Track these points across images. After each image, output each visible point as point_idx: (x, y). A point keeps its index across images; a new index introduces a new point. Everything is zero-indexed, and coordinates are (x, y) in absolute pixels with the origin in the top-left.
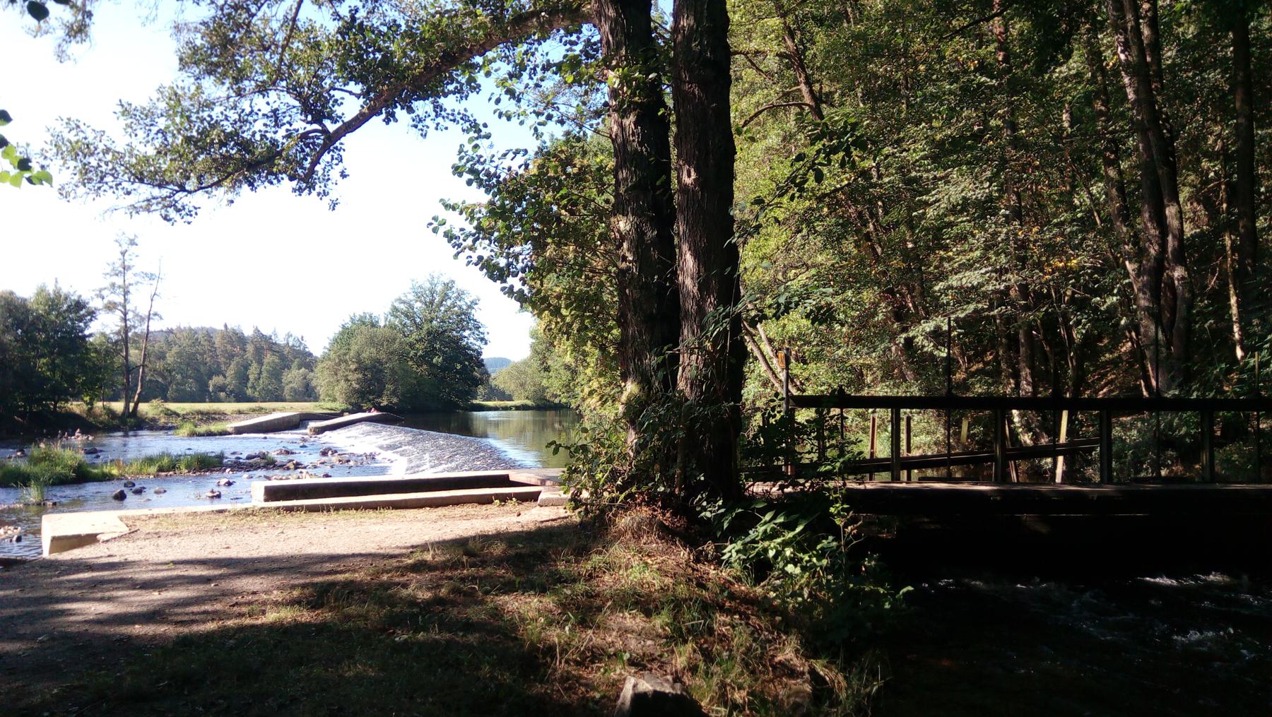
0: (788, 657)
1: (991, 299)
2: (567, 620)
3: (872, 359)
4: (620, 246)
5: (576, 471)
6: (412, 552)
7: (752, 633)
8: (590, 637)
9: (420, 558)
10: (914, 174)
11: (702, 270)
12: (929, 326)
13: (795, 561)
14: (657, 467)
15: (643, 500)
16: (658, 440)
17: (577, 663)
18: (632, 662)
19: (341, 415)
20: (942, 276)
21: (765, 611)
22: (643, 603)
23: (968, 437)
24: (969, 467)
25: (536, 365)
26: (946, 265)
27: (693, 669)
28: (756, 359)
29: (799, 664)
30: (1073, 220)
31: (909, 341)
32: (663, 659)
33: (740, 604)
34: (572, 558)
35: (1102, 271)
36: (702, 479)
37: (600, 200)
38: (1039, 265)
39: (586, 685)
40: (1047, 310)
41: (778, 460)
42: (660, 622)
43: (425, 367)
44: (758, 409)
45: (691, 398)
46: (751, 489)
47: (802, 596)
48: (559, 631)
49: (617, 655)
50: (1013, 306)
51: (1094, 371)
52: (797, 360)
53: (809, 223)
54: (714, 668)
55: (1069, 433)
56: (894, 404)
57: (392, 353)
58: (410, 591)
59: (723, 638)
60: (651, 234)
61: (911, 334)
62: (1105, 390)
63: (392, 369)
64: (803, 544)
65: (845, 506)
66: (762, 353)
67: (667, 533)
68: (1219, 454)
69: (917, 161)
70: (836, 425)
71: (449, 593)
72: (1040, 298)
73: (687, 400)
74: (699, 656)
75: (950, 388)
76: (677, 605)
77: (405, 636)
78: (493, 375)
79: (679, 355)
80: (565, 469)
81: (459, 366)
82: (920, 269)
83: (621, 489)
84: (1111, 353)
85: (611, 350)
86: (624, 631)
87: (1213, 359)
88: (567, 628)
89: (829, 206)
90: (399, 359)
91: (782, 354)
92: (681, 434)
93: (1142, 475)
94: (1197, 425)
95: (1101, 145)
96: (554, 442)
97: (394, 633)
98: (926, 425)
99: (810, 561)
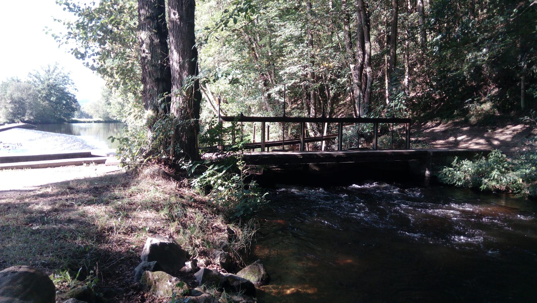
0: (218, 224)
1: (301, 78)
2: (119, 215)
3: (255, 102)
4: (141, 46)
5: (123, 150)
6: (41, 188)
7: (204, 215)
8: (131, 222)
9: (45, 191)
10: (271, 23)
11: (181, 58)
12: (277, 89)
13: (222, 185)
14: (162, 147)
15: (156, 162)
16: (162, 135)
17: (124, 233)
18: (151, 231)
19: (4, 124)
20: (282, 68)
21: (209, 206)
22: (155, 206)
23: (291, 134)
24: (291, 146)
25: (104, 102)
26: (284, 63)
27: (178, 232)
28: (206, 101)
29: (223, 226)
30: (332, 47)
31: (269, 95)
32: (164, 229)
33: (199, 204)
34: (122, 188)
35: (341, 68)
36: (182, 152)
37: (132, 24)
38: (319, 65)
39: (128, 243)
40: (321, 84)
41: (215, 143)
42: (163, 214)
43: (47, 102)
44: (207, 123)
45: (177, 116)
46: (204, 156)
47: (225, 199)
48: (115, 220)
49: (143, 229)
50: (309, 81)
51: (337, 108)
52: (224, 102)
53: (229, 42)
54: (188, 231)
55: (327, 131)
56: (263, 120)
57: (29, 95)
58: (40, 206)
59: (191, 218)
60: (157, 41)
61: (270, 92)
62: (340, 115)
63: (30, 103)
64: (226, 178)
65: (243, 162)
66: (209, 99)
67: (166, 176)
68: (379, 139)
69: (273, 17)
70: (240, 128)
71: (60, 206)
72: (319, 78)
73: (175, 117)
74: (180, 226)
75: (284, 114)
76: (171, 206)
77: (38, 227)
78: (82, 107)
79: (171, 97)
80: (118, 149)
81: (64, 102)
82: (274, 64)
83: (145, 157)
84: (343, 101)
85: (140, 95)
86: (146, 219)
87: (379, 104)
88: (119, 219)
89: (237, 35)
90: (33, 98)
91: (217, 98)
92: (173, 132)
93: (353, 147)
94: (372, 128)
95: (343, 16)
96: (112, 137)
97: (32, 225)
98: (275, 129)
99: (228, 185)
